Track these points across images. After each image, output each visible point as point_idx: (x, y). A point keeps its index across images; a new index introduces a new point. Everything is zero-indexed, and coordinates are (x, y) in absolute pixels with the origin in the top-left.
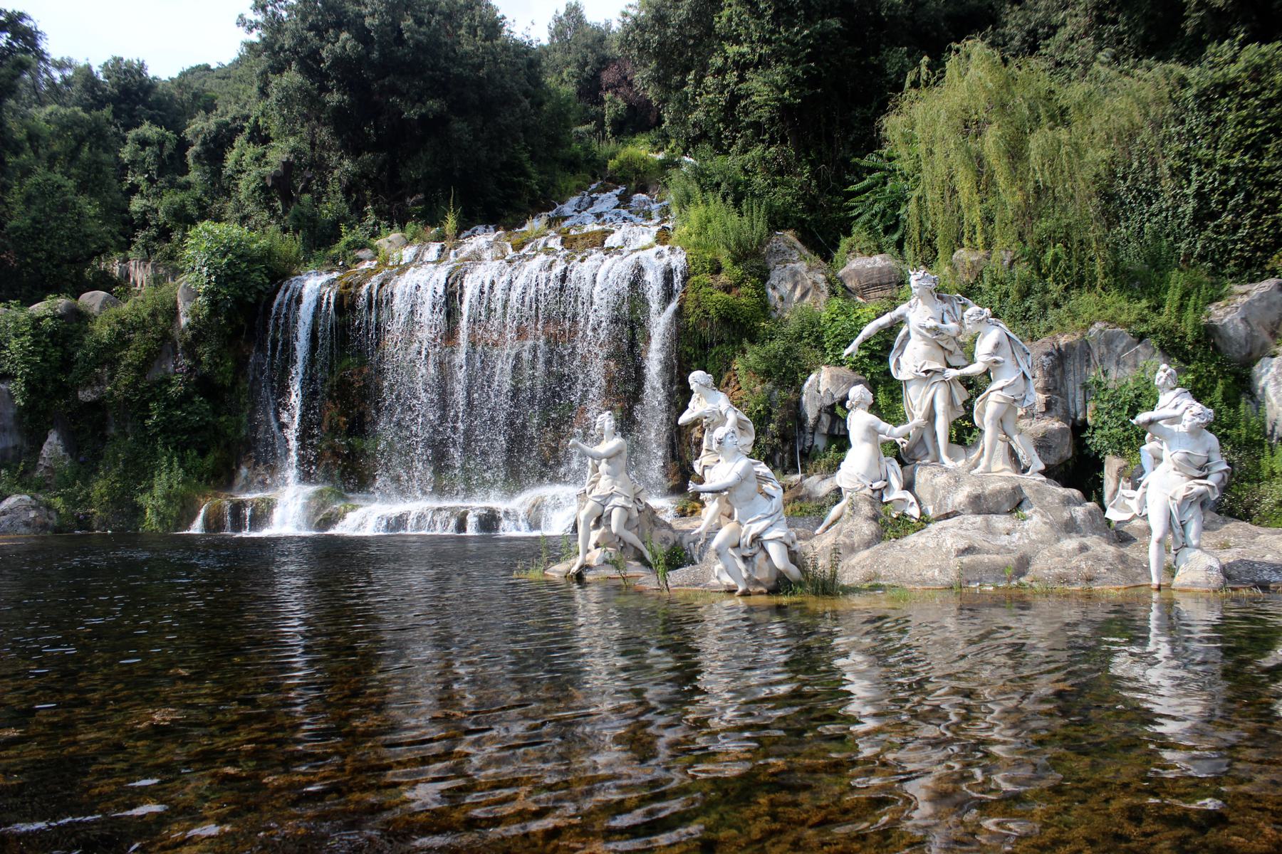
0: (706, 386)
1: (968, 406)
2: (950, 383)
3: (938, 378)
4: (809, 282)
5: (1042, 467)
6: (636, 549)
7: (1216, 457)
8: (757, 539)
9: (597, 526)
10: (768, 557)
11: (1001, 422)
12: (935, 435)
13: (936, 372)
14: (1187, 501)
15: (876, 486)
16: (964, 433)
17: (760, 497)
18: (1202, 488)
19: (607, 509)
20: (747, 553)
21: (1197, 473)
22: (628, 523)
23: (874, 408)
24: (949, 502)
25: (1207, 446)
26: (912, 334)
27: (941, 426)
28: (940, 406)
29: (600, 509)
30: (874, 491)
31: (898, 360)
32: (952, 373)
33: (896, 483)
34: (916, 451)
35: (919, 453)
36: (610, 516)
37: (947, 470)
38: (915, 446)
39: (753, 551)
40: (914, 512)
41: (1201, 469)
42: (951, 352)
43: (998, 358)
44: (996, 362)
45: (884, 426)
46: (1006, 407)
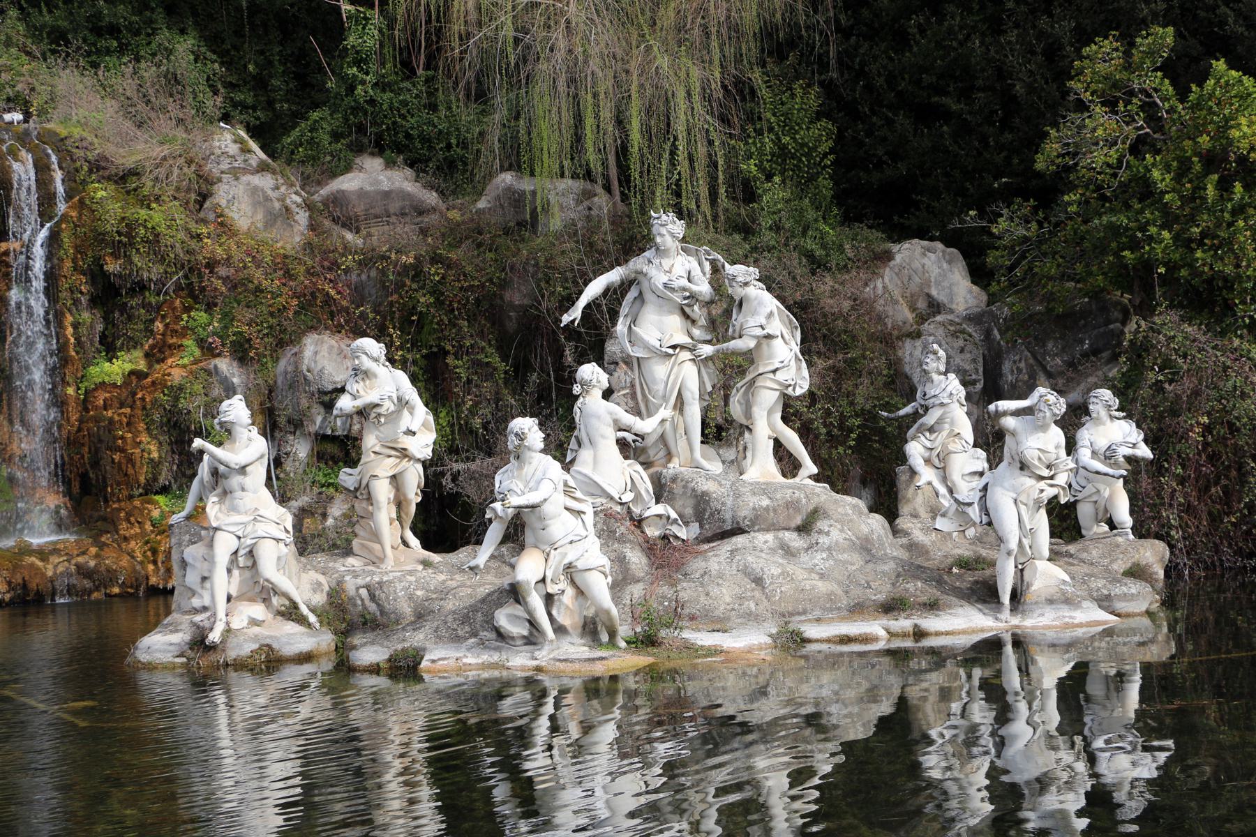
13: (683, 347)
32: (707, 350)
41: (1049, 467)
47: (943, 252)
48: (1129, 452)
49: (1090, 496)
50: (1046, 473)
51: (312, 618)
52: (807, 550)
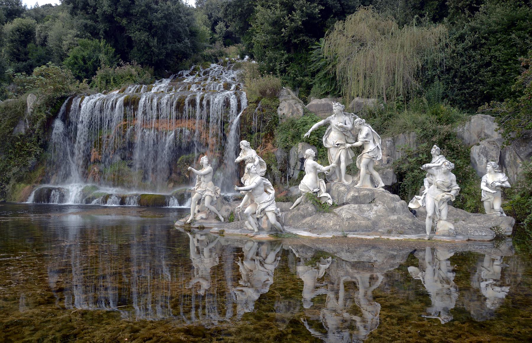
0: (247, 147)
1: (354, 159)
2: (347, 149)
3: (342, 147)
4: (295, 108)
5: (383, 185)
6: (215, 213)
7: (455, 183)
8: (263, 210)
9: (198, 204)
10: (267, 218)
11: (367, 166)
12: (340, 170)
13: (341, 144)
14: (442, 201)
15: (315, 190)
16: (352, 170)
17: (265, 193)
18: (448, 196)
19: (203, 196)
20: (259, 216)
21: (446, 190)
22: (212, 202)
23: (316, 158)
24: (345, 198)
25: (451, 178)
26: (333, 129)
27: (343, 166)
28: (343, 158)
29: (200, 196)
30: (314, 192)
31: (326, 139)
32: (348, 145)
33: (323, 190)
34: (332, 177)
35: (333, 177)
36: (204, 199)
37: (344, 185)
38: (332, 175)
39: (261, 216)
40: (330, 202)
41: (448, 188)
42: (348, 137)
43: (367, 140)
44: (366, 141)
45: (319, 166)
46: (369, 160)
47: (490, 118)
48: (499, 184)
49: (487, 199)
50: (446, 190)
51: (222, 219)
52: (368, 211)
